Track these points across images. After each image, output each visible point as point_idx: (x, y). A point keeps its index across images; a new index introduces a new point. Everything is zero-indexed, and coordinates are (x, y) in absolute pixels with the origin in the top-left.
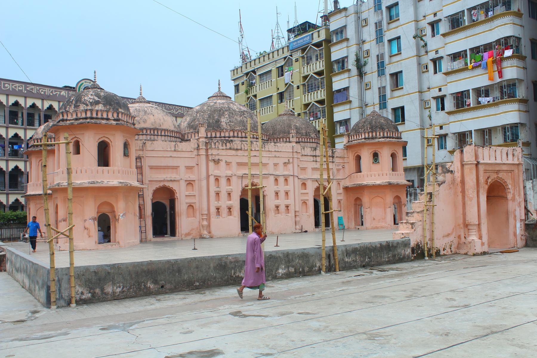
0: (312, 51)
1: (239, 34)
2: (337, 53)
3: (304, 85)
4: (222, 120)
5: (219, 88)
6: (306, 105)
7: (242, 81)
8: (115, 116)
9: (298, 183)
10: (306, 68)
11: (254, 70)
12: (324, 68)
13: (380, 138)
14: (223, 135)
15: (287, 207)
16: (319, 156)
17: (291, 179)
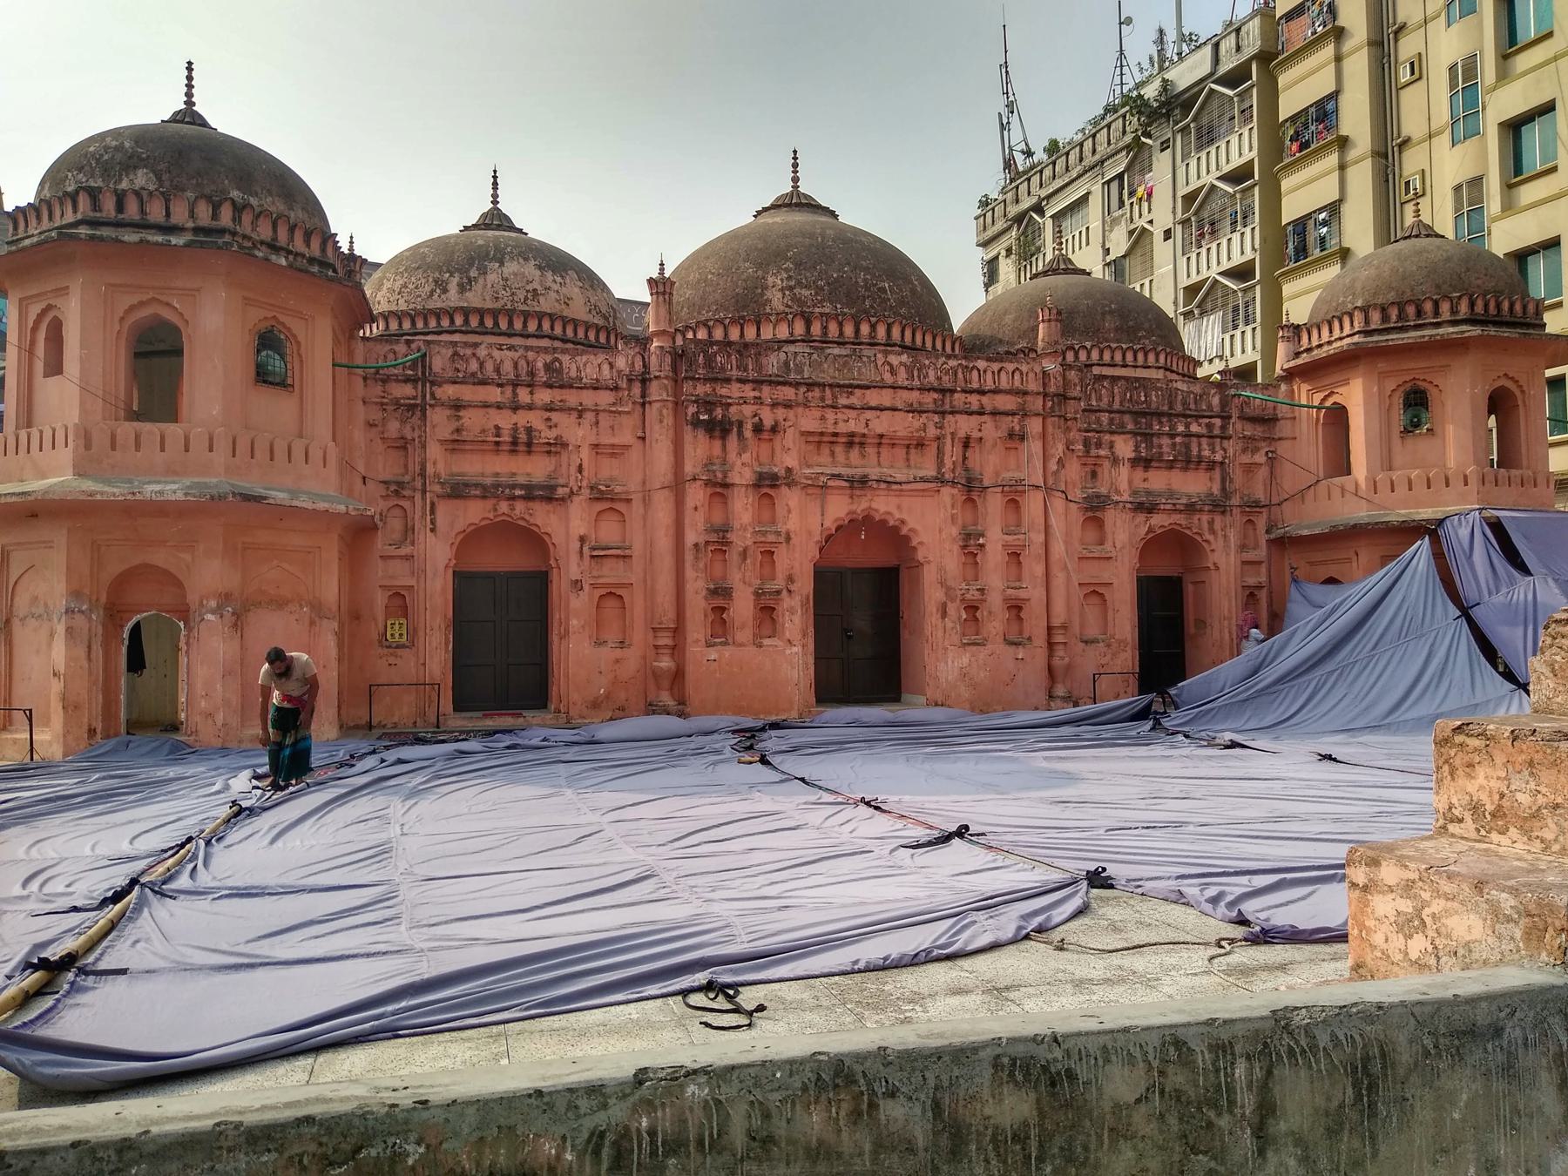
0: (1215, 103)
1: (1002, 101)
2: (1299, 89)
3: (1185, 222)
4: (770, 280)
5: (795, 180)
6: (1192, 291)
7: (1005, 245)
8: (204, 213)
9: (1065, 519)
10: (1193, 164)
11: (1041, 200)
12: (1255, 153)
13: (1438, 325)
14: (767, 333)
15: (1016, 608)
16: (1160, 415)
17: (1033, 505)
